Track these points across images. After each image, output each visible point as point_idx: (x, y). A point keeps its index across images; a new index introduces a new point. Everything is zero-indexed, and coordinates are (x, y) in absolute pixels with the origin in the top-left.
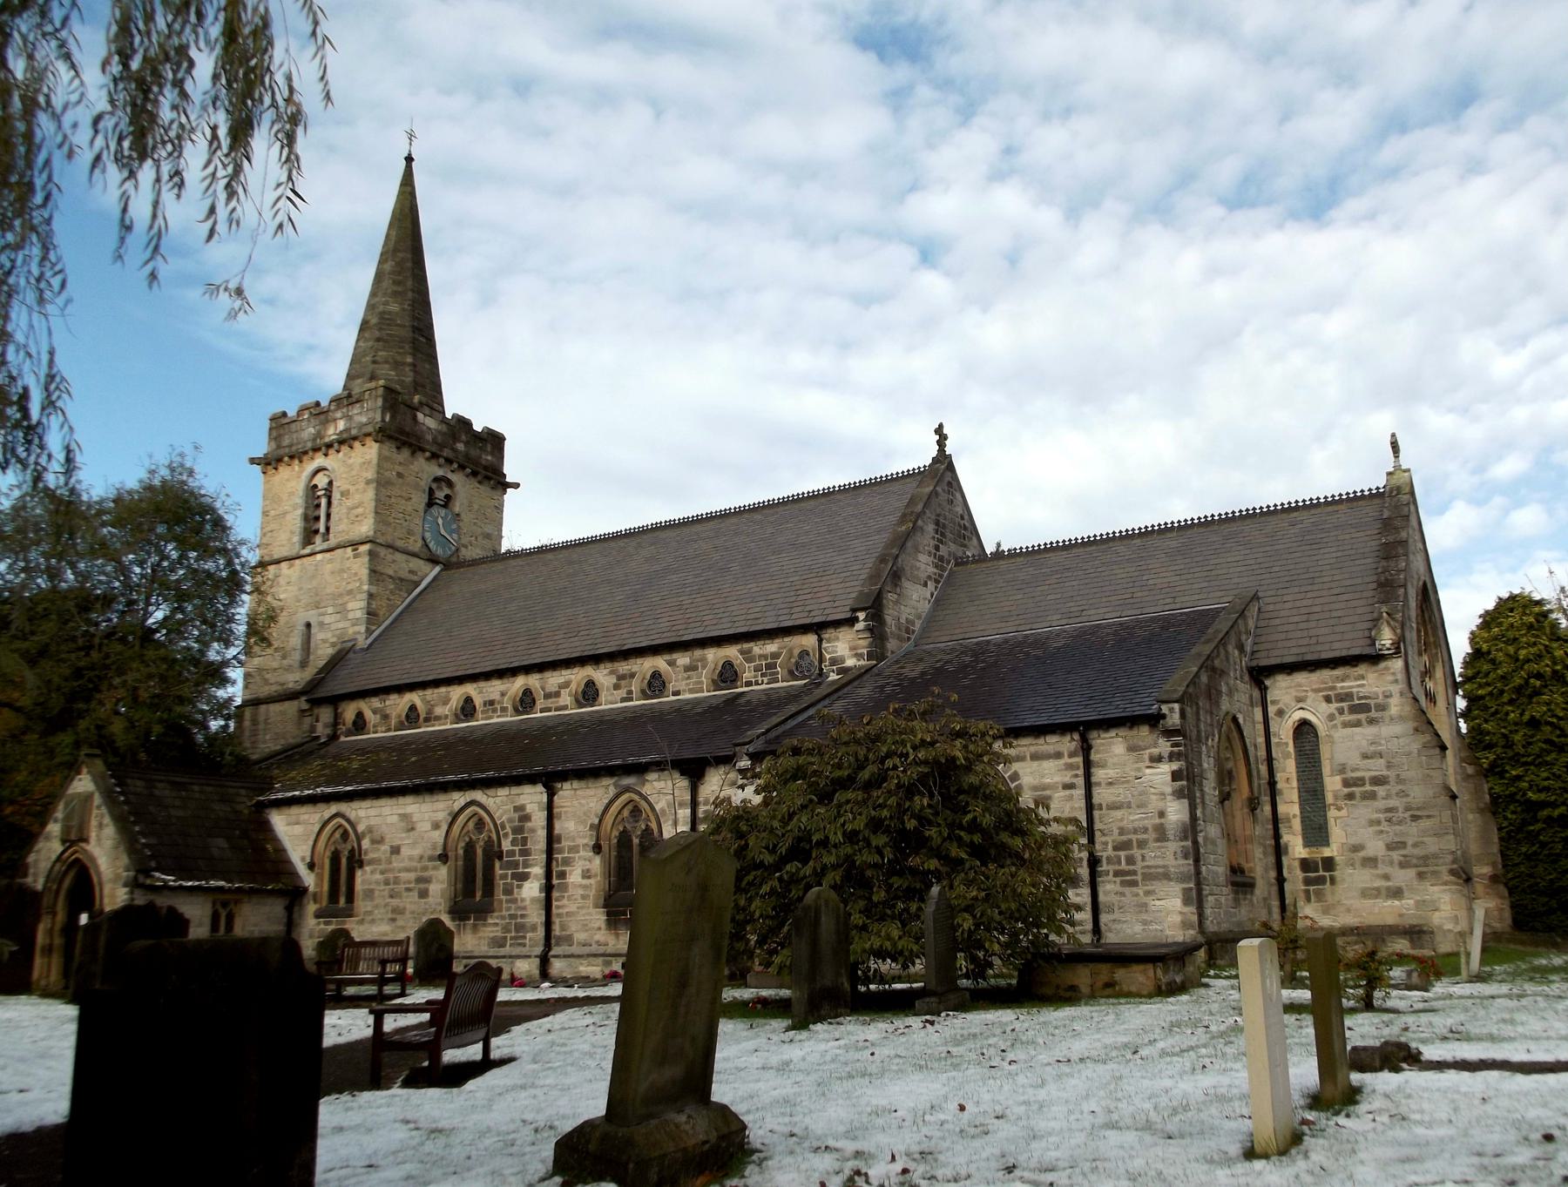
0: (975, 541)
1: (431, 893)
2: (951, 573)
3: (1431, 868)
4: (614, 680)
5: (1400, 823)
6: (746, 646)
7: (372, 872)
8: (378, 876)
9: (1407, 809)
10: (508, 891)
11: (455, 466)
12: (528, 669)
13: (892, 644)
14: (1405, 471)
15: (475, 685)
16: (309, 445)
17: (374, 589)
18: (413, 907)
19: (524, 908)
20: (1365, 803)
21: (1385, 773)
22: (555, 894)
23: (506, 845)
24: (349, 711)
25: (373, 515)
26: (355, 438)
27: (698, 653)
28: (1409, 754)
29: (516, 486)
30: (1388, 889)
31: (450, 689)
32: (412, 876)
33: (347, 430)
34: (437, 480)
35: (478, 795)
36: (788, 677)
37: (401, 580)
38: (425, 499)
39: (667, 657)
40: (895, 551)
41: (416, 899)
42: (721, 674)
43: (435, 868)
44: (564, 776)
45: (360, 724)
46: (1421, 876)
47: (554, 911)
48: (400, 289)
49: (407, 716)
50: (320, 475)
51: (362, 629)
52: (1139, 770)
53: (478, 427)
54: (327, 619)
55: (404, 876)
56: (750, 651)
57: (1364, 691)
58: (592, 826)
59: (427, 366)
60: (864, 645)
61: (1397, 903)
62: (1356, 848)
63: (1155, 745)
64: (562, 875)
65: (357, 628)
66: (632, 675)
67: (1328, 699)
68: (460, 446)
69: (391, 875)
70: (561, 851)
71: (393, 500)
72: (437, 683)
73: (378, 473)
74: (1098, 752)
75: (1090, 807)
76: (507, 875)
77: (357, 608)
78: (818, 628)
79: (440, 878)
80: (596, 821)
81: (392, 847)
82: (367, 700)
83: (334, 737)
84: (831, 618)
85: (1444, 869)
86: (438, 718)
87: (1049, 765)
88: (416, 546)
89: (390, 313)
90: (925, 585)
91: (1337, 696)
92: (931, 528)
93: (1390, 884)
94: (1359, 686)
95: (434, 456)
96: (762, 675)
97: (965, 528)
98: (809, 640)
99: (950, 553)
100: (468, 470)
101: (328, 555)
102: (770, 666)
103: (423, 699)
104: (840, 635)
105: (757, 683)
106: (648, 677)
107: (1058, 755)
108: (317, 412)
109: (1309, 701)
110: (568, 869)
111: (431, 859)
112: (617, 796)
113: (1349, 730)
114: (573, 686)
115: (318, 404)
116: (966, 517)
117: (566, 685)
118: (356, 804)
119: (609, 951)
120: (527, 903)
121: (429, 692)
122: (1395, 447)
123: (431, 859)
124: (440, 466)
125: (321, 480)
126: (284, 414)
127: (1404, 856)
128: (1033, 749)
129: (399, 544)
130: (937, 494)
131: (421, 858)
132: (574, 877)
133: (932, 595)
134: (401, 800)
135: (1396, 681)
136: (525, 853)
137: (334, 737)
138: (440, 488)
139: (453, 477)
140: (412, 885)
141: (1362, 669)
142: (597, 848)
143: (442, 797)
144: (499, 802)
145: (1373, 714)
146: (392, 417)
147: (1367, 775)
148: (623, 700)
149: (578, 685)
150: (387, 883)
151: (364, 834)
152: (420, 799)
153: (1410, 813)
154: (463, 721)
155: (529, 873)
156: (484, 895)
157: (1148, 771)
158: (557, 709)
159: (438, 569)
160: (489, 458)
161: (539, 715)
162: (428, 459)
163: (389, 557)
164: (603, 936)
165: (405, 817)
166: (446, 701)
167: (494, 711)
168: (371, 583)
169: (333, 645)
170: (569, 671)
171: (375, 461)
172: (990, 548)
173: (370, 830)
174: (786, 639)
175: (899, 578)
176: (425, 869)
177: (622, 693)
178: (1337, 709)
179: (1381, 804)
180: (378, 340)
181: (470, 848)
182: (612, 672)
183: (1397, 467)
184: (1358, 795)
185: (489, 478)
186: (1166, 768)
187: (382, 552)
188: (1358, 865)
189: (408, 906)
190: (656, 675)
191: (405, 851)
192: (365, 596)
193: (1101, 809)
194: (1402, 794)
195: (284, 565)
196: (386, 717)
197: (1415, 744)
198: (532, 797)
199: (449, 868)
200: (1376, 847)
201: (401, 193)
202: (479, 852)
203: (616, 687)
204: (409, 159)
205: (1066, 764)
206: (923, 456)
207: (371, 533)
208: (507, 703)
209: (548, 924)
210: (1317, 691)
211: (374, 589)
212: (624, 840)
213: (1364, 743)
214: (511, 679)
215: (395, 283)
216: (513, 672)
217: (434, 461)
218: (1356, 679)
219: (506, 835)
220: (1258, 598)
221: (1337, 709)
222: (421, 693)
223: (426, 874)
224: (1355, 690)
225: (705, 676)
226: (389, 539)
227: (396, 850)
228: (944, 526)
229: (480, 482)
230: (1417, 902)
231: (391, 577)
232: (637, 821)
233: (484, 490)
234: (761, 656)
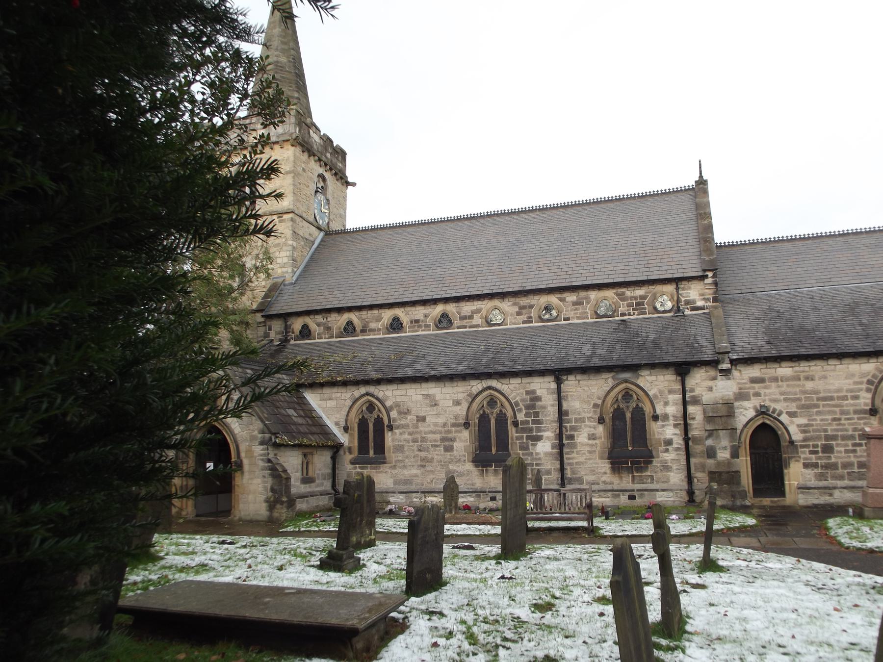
1: (455, 448)
4: (516, 309)
6: (620, 290)
7: (401, 434)
8: (406, 436)
10: (524, 447)
11: (328, 167)
12: (446, 300)
15: (402, 309)
17: (295, 244)
18: (439, 458)
19: (540, 459)
22: (565, 450)
23: (521, 417)
24: (297, 324)
25: (292, 194)
27: (583, 294)
29: (354, 184)
31: (381, 311)
32: (438, 436)
35: (494, 383)
36: (653, 311)
39: (559, 296)
41: (443, 452)
43: (460, 432)
44: (569, 371)
45: (306, 333)
47: (565, 461)
48: (286, 47)
49: (345, 328)
51: (290, 270)
55: (430, 436)
56: (623, 294)
58: (595, 406)
60: (709, 293)
64: (571, 437)
65: (285, 269)
66: (531, 307)
69: (419, 436)
70: (569, 421)
72: (371, 307)
76: (522, 438)
78: (677, 281)
79: (463, 438)
80: (600, 402)
81: (417, 417)
82: (312, 317)
83: (285, 341)
84: (686, 275)
86: (372, 330)
88: (311, 219)
89: (281, 63)
98: (670, 288)
102: (638, 304)
103: (360, 318)
104: (692, 286)
105: (629, 314)
110: (576, 433)
111: (454, 425)
114: (484, 312)
117: (478, 311)
118: (382, 387)
119: (615, 488)
120: (542, 455)
123: (454, 425)
129: (304, 215)
131: (445, 425)
132: (582, 438)
134: (424, 385)
136: (538, 422)
137: (285, 341)
139: (327, 175)
140: (439, 443)
142: (601, 420)
143: (461, 383)
144: (513, 389)
148: (524, 322)
150: (415, 441)
151: (391, 408)
152: (442, 384)
154: (393, 333)
155: (542, 436)
156: (497, 451)
158: (470, 327)
161: (456, 330)
162: (315, 161)
164: (608, 477)
165: (427, 396)
166: (379, 319)
167: (420, 327)
170: (480, 302)
171: (292, 158)
173: (397, 405)
174: (651, 287)
176: (449, 432)
177: (524, 317)
181: (484, 419)
182: (514, 304)
189: (435, 457)
191: (428, 419)
192: (290, 248)
196: (328, 329)
198: (543, 387)
199: (470, 432)
202: (493, 422)
203: (519, 314)
206: (690, 181)
208: (429, 321)
209: (562, 470)
211: (295, 244)
212: (618, 415)
214: (432, 306)
215: (283, 43)
216: (435, 302)
217: (318, 164)
219: (520, 410)
222: (357, 313)
223: (450, 436)
227: (422, 419)
229: (337, 180)
231: (302, 237)
232: (628, 402)
233: (339, 184)
234: (631, 298)
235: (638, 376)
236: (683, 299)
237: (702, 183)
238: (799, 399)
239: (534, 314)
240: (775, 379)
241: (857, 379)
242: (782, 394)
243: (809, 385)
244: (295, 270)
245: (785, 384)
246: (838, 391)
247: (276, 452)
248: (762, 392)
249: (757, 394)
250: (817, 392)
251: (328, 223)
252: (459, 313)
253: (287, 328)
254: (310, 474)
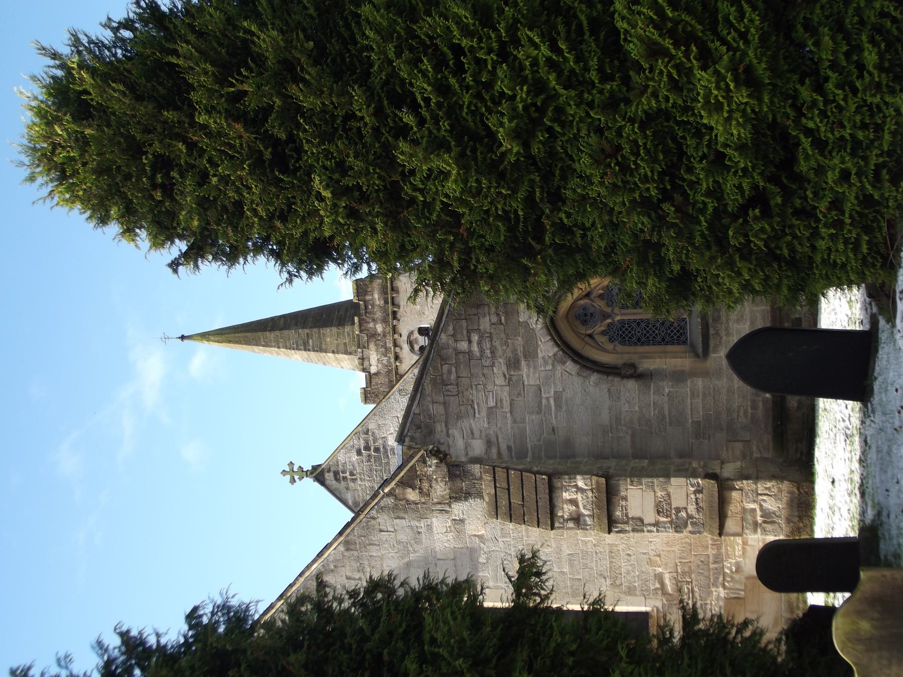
11: (396, 336)
68: (379, 328)
95: (397, 358)
100: (395, 322)
160: (376, 296)
162: (401, 362)
185: (393, 298)
217: (401, 356)
229: (399, 307)
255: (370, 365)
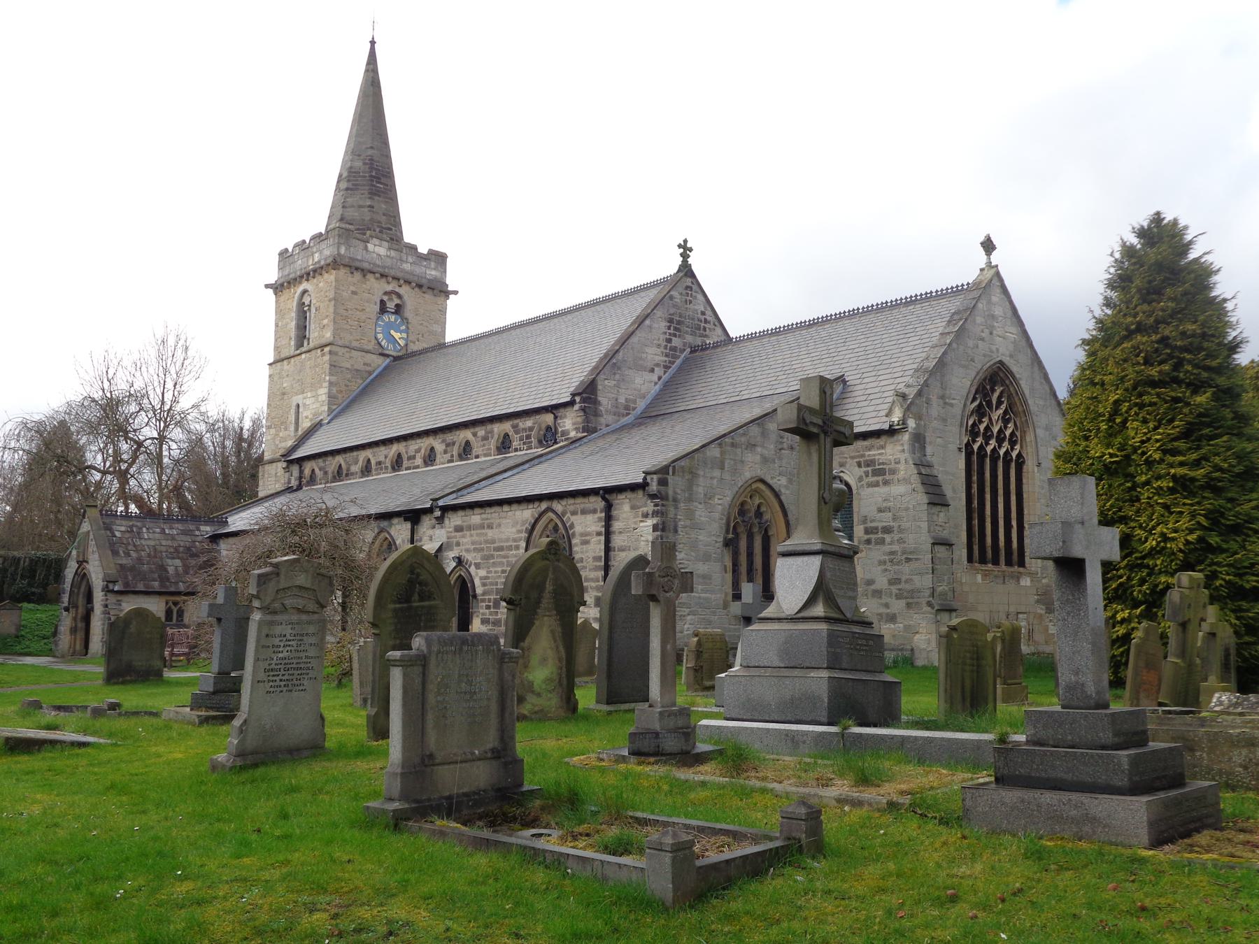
0: (719, 331)
2: (686, 360)
3: (915, 600)
5: (899, 563)
6: (516, 421)
9: (904, 553)
13: (606, 419)
14: (993, 267)
15: (371, 450)
16: (298, 273)
17: (334, 379)
20: (878, 547)
21: (892, 524)
24: (308, 467)
26: (322, 268)
27: (489, 427)
28: (907, 509)
29: (456, 293)
30: (887, 614)
31: (358, 453)
33: (319, 262)
34: (386, 293)
36: (537, 445)
37: (357, 370)
38: (377, 308)
39: (472, 430)
40: (618, 348)
42: (503, 443)
46: (909, 605)
50: (306, 294)
52: (635, 523)
53: (423, 250)
54: (308, 402)
57: (882, 459)
59: (384, 206)
61: (892, 626)
62: (870, 582)
63: (645, 505)
66: (454, 444)
67: (859, 465)
71: (350, 312)
73: (335, 293)
74: (615, 510)
75: (608, 549)
77: (323, 392)
78: (553, 409)
85: (924, 601)
87: (590, 518)
88: (371, 346)
90: (652, 371)
91: (867, 461)
92: (663, 325)
93: (888, 611)
94: (880, 454)
96: (524, 444)
97: (706, 321)
98: (548, 418)
99: (685, 344)
101: (308, 355)
103: (347, 463)
105: (520, 450)
106: (463, 444)
107: (595, 511)
108: (301, 245)
109: (848, 466)
112: (379, 533)
113: (871, 489)
114: (423, 451)
115: (304, 242)
116: (709, 312)
117: (418, 451)
121: (348, 455)
122: (988, 246)
124: (388, 283)
125: (306, 300)
126: (286, 250)
127: (900, 590)
128: (582, 506)
129: (355, 344)
130: (671, 298)
133: (660, 378)
135: (903, 451)
138: (391, 299)
139: (401, 291)
141: (881, 441)
145: (887, 477)
146: (346, 249)
147: (880, 525)
149: (426, 450)
153: (905, 556)
157: (642, 524)
159: (388, 360)
160: (433, 273)
162: (377, 279)
163: (347, 355)
167: (381, 469)
168: (331, 374)
169: (311, 420)
171: (334, 284)
172: (733, 333)
174: (537, 417)
175: (619, 368)
177: (448, 456)
178: (865, 472)
179: (887, 548)
180: (347, 189)
182: (443, 441)
183: (989, 264)
184: (873, 540)
186: (650, 522)
187: (341, 351)
188: (869, 596)
190: (468, 443)
192: (326, 384)
193: (614, 551)
194: (901, 541)
195: (285, 362)
196: (326, 473)
197: (923, 498)
200: (882, 582)
201: (367, 71)
203: (445, 452)
204: (373, 43)
205: (598, 518)
206: (671, 266)
207: (332, 338)
210: (852, 458)
211: (334, 379)
213: (880, 499)
217: (384, 280)
218: (878, 449)
220: (844, 382)
221: (865, 472)
224: (877, 457)
225: (493, 444)
226: (347, 344)
228: (679, 323)
230: (905, 626)
231: (347, 369)
233: (428, 297)
234: (523, 429)
235: (391, 525)
236: (560, 430)
237: (686, 270)
238: (482, 549)
239: (455, 453)
240: (469, 528)
241: (519, 527)
242: (473, 543)
243: (490, 534)
244: (334, 407)
245: (475, 532)
246: (507, 540)
247: (120, 598)
248: (462, 540)
249: (458, 544)
250: (493, 542)
251: (406, 345)
252: (407, 453)
253: (301, 472)
254: (186, 620)
255: (375, 245)
